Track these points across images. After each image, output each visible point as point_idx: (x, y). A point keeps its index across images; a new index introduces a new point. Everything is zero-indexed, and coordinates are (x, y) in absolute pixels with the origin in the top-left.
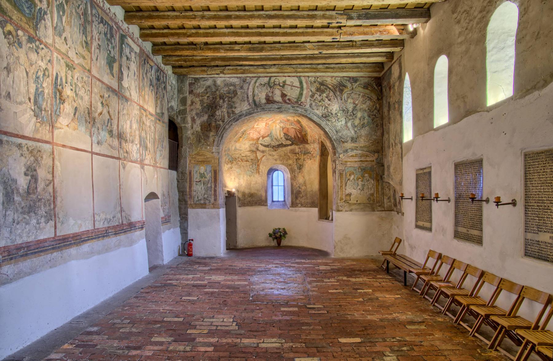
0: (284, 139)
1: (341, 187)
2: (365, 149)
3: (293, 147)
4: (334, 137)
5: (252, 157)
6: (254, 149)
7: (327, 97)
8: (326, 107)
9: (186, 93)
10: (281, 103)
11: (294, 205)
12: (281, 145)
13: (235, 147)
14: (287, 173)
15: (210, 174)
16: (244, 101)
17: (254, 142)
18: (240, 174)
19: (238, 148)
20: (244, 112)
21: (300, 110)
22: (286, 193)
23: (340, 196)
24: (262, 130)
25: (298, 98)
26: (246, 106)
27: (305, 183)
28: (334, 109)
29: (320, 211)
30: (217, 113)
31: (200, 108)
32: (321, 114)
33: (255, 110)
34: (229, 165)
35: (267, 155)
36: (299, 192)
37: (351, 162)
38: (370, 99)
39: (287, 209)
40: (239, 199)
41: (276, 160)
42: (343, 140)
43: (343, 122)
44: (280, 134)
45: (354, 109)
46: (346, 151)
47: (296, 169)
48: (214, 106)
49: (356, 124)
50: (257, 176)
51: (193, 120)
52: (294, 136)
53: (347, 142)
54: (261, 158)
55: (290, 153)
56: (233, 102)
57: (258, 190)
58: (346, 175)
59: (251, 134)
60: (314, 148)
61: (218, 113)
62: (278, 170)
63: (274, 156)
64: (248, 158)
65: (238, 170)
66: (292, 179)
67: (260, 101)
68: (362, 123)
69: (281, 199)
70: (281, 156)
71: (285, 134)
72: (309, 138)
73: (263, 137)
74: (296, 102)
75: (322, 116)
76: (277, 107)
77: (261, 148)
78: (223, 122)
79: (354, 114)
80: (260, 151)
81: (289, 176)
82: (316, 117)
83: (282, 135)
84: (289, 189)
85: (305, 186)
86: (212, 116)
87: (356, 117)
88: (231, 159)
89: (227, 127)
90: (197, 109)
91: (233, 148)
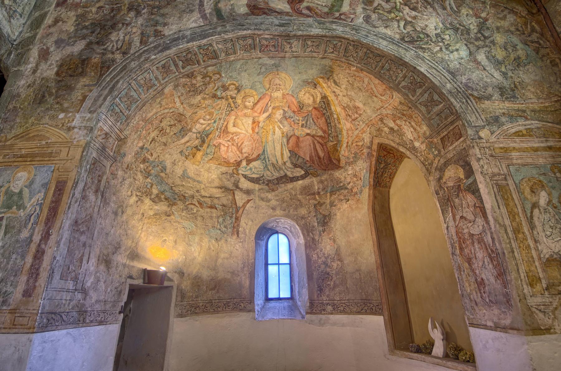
0: (289, 164)
1: (517, 230)
2: (549, 117)
3: (307, 181)
4: (448, 86)
5: (224, 201)
6: (230, 185)
7: (406, 5)
8: (407, 23)
9: (50, 6)
10: (287, 14)
11: (315, 307)
12: (285, 179)
13: (185, 171)
14: (296, 236)
15: (42, 195)
16: (192, 11)
17: (230, 170)
18: (192, 233)
19: (191, 174)
20: (188, 33)
21: (341, 29)
22: (296, 279)
23: (523, 269)
24: (246, 143)
25: (333, 6)
26: (195, 21)
27: (338, 252)
28: (432, 26)
29: (392, 324)
30: (113, 37)
31: (72, 29)
32: (397, 36)
33: (219, 29)
34: (162, 207)
35: (257, 199)
36: (326, 276)
37: (519, 150)
38: (512, 11)
39: (299, 317)
40: (182, 295)
41: (274, 209)
42: (475, 94)
43: (464, 53)
44: (282, 154)
45: (482, 26)
46: (495, 121)
47: (315, 224)
48: (109, 23)
49: (500, 58)
50: (233, 240)
51: (44, 55)
52: (311, 157)
53: (489, 98)
54: (244, 206)
55: (301, 193)
56: (163, 15)
57: (233, 273)
58: (520, 192)
59: (223, 148)
60: (357, 172)
61: (117, 37)
62: (277, 232)
63: (269, 201)
64: (216, 201)
65: (186, 223)
66: (307, 246)
67: (233, 9)
68: (512, 56)
69: (285, 293)
70: (283, 201)
71: (293, 154)
72: (344, 152)
73: (249, 161)
74: (327, 14)
75: (403, 39)
76: (277, 22)
77: (245, 184)
78: (124, 53)
79: (485, 38)
80: (241, 190)
81: (302, 241)
82: (385, 43)
83: (287, 154)
84: (301, 269)
85: (340, 260)
86: (98, 43)
87: (493, 42)
88: (168, 194)
89: (133, 65)
90: (61, 32)
91: (179, 171)
